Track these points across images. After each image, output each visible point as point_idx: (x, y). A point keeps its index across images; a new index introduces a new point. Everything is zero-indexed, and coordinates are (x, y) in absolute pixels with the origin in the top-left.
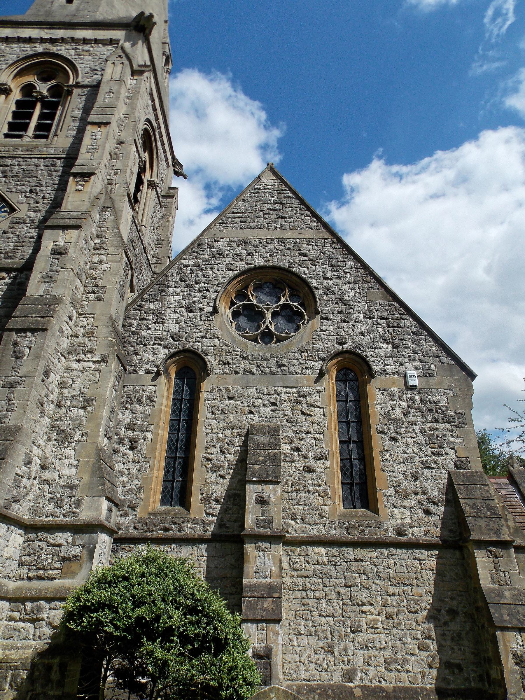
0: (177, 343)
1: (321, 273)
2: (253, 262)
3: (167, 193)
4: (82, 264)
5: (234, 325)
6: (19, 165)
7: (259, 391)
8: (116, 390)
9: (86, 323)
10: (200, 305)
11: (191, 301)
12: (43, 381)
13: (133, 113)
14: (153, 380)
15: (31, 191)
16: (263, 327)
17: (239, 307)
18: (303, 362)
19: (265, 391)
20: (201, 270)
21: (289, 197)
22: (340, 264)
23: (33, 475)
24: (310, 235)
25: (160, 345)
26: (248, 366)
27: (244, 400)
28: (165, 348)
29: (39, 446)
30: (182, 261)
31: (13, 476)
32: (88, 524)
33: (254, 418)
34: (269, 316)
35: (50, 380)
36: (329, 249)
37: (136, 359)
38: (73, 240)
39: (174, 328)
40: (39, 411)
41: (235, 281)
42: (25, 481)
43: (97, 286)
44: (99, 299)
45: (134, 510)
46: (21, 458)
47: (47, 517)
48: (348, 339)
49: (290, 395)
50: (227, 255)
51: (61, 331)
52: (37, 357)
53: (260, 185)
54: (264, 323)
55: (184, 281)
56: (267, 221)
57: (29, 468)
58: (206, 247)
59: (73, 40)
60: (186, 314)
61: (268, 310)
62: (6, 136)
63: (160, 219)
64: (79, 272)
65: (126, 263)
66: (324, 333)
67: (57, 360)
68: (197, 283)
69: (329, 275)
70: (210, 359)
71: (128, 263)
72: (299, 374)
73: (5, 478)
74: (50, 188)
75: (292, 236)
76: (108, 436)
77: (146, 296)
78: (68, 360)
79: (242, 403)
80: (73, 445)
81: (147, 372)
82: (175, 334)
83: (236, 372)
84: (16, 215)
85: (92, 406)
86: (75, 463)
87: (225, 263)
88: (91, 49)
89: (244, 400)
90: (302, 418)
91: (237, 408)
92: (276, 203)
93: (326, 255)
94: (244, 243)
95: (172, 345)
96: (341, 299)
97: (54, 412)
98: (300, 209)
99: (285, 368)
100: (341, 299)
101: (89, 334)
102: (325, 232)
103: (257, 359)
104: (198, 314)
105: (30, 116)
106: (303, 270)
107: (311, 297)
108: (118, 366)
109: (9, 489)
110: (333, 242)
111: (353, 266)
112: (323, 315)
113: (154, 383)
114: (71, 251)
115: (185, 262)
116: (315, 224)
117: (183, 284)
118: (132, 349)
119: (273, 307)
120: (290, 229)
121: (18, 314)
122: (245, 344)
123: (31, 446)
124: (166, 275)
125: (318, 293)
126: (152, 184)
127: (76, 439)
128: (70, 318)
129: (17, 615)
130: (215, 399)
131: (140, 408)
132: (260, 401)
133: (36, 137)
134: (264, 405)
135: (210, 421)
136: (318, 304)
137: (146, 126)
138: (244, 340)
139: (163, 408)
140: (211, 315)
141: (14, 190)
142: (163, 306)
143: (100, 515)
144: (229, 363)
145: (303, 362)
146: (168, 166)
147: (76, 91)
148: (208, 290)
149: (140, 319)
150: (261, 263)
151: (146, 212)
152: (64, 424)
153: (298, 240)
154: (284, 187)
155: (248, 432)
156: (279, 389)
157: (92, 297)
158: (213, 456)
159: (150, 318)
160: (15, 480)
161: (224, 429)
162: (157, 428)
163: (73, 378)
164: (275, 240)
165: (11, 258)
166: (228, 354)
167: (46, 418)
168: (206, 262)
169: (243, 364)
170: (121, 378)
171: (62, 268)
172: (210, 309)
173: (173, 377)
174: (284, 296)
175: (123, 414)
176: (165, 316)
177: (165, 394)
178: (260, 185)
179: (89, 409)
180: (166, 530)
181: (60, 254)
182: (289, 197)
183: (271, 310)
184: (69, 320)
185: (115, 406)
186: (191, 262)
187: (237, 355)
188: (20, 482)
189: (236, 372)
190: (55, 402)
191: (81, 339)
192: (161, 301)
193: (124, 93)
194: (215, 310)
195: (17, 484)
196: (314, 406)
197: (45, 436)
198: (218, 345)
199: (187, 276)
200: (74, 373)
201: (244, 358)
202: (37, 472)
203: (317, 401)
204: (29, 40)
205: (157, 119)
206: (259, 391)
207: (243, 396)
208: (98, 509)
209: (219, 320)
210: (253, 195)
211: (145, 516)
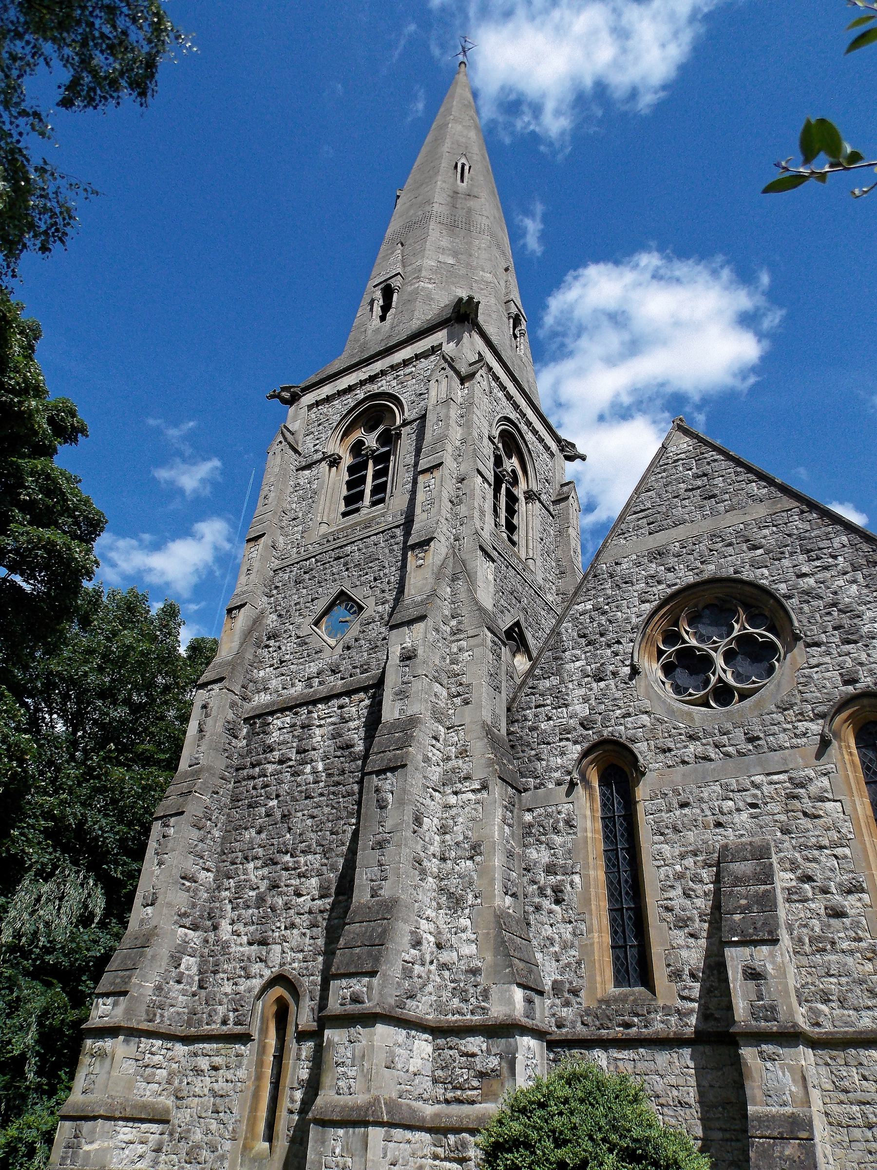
0: (591, 732)
1: (791, 570)
2: (678, 581)
3: (559, 495)
4: (437, 662)
5: (668, 686)
6: (359, 550)
7: (726, 787)
8: (509, 825)
9: (456, 739)
10: (611, 668)
11: (599, 665)
12: (415, 832)
13: (470, 434)
14: (569, 793)
15: (375, 579)
16: (713, 679)
17: (670, 656)
18: (790, 726)
19: (734, 787)
20: (604, 613)
21: (715, 461)
22: (822, 546)
23: (428, 958)
24: (761, 511)
25: (568, 739)
26: (700, 749)
27: (704, 806)
28: (576, 743)
29: (427, 919)
30: (576, 607)
31: (399, 964)
32: (500, 1024)
33: (725, 833)
34: (719, 661)
35: (425, 827)
36: (798, 524)
37: (540, 766)
38: (421, 636)
39: (582, 710)
40: (417, 873)
41: (656, 618)
42: (417, 969)
43: (461, 684)
44: (466, 702)
45: (578, 996)
46: (407, 939)
47: (453, 1015)
48: (861, 672)
49: (777, 786)
50: (637, 580)
51: (427, 760)
52: (401, 803)
53: (668, 458)
54: (714, 674)
55: (584, 636)
56: (687, 509)
57: (420, 950)
58: (605, 576)
59: (393, 368)
60: (594, 685)
61: (715, 650)
62: (345, 514)
63: (556, 536)
64: (436, 674)
65: (493, 642)
66: (816, 669)
67: (429, 800)
68: (602, 635)
69: (805, 569)
70: (640, 748)
71: (496, 639)
72: (787, 748)
73: (389, 969)
74: (393, 569)
75: (731, 522)
76: (509, 893)
77: (538, 672)
78: (443, 793)
79: (703, 811)
80: (467, 911)
81: (559, 784)
82: (585, 718)
83: (684, 762)
84: (365, 615)
85: (480, 854)
86: (473, 937)
87: (636, 594)
88: (414, 369)
89: (704, 806)
90: (805, 822)
91: (695, 820)
92: (696, 477)
93: (795, 537)
94: (658, 555)
95: (584, 737)
96: (834, 605)
97: (439, 869)
98: (737, 474)
99: (760, 742)
100: (834, 605)
101: (463, 753)
102: (785, 498)
103: (713, 735)
104: (612, 682)
105: (363, 479)
106: (758, 572)
107: (782, 613)
108: (506, 790)
109: (398, 982)
110: (802, 512)
111: (846, 542)
112: (808, 640)
113: (570, 799)
114: (420, 652)
115: (580, 607)
116: (765, 491)
117: (583, 641)
118: (533, 752)
119: (723, 644)
120: (727, 512)
121: (375, 750)
122: (689, 714)
123: (417, 921)
124: (559, 634)
125: (791, 604)
126: (530, 496)
127: (470, 903)
128: (436, 738)
129: (440, 1151)
130: (661, 811)
131: (558, 840)
132: (731, 803)
133: (374, 504)
134: (738, 810)
135: (658, 846)
136: (796, 624)
137: (503, 427)
138: (686, 707)
139: (589, 835)
140: (631, 679)
141: (358, 583)
142: (562, 682)
143: (514, 1011)
144: (670, 750)
145: (790, 726)
146: (552, 455)
147: (405, 431)
148: (619, 642)
149: (536, 707)
150: (691, 579)
152: (453, 883)
153: (742, 526)
154: (704, 449)
155: (719, 857)
156: (758, 779)
157: (457, 701)
158: (673, 903)
159: (548, 702)
160: (403, 969)
161: (682, 856)
162: (586, 866)
163: (453, 818)
164: (705, 537)
165: (366, 671)
166: (666, 735)
167: (430, 879)
168: (609, 600)
169: (693, 748)
170: (514, 806)
171: (414, 677)
172: (627, 670)
173: (596, 784)
174: (737, 622)
175: (538, 852)
176: (567, 694)
177: (588, 813)
178: (668, 458)
179: (478, 859)
180: (627, 1026)
181: (409, 658)
182: (715, 461)
183: (721, 650)
184: (434, 742)
185: (512, 847)
187: (681, 734)
188: (411, 971)
189: (684, 762)
190: (438, 854)
191: (453, 763)
192: (558, 673)
193: (454, 412)
194: (635, 671)
195: (407, 973)
196: (822, 800)
197: (434, 904)
198: (649, 724)
199: (586, 628)
200: (454, 812)
201: (692, 738)
202: (432, 953)
203: (826, 791)
204: (350, 389)
205: (516, 407)
206: (726, 787)
207: (701, 800)
208: (510, 1001)
209: (643, 684)
210: (660, 476)
211: (594, 1005)
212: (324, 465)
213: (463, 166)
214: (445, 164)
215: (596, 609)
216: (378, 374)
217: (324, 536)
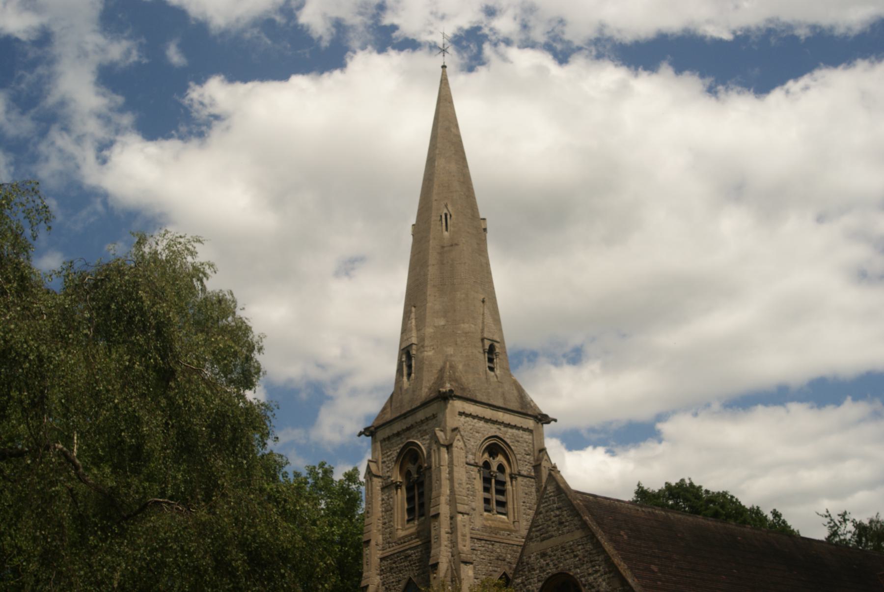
92: (558, 509)
94: (544, 555)
150: (554, 571)
151: (515, 506)
186: (520, 581)
212: (393, 487)
213: (446, 215)
214: (434, 218)
215: (522, 583)
216: (410, 427)
217: (400, 539)
